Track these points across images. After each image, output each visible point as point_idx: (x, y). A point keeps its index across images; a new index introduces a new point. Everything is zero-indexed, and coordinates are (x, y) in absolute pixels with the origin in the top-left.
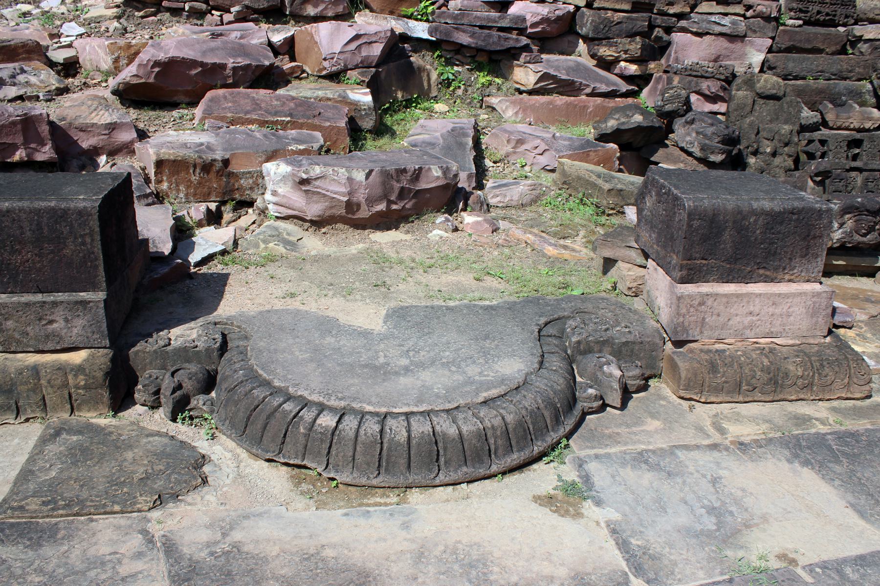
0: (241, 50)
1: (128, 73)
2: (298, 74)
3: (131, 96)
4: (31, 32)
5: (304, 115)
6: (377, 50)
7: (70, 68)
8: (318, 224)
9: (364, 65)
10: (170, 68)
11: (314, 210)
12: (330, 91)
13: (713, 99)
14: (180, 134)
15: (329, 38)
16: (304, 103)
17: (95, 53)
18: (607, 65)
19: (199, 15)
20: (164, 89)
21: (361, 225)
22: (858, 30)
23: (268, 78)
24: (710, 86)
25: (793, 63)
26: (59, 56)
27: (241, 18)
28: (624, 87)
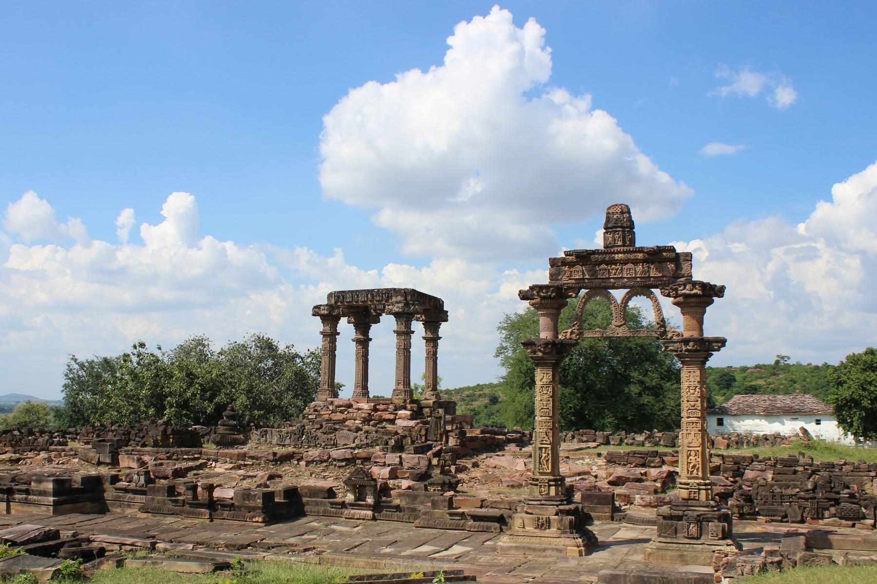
0: (634, 474)
1: (611, 479)
2: (647, 480)
3: (611, 483)
4: (586, 469)
5: (646, 488)
6: (665, 475)
7: (596, 477)
8: (644, 506)
9: (662, 478)
10: (619, 478)
11: (644, 503)
12: (652, 483)
13: (749, 486)
14: (618, 490)
15: (654, 472)
16: (646, 486)
17: (602, 473)
18: (727, 479)
19: (625, 465)
20: (618, 482)
21: (652, 507)
22: (796, 469)
23: (639, 480)
24: (749, 483)
25: (779, 477)
26: (594, 474)
27: (635, 466)
28: (730, 483)
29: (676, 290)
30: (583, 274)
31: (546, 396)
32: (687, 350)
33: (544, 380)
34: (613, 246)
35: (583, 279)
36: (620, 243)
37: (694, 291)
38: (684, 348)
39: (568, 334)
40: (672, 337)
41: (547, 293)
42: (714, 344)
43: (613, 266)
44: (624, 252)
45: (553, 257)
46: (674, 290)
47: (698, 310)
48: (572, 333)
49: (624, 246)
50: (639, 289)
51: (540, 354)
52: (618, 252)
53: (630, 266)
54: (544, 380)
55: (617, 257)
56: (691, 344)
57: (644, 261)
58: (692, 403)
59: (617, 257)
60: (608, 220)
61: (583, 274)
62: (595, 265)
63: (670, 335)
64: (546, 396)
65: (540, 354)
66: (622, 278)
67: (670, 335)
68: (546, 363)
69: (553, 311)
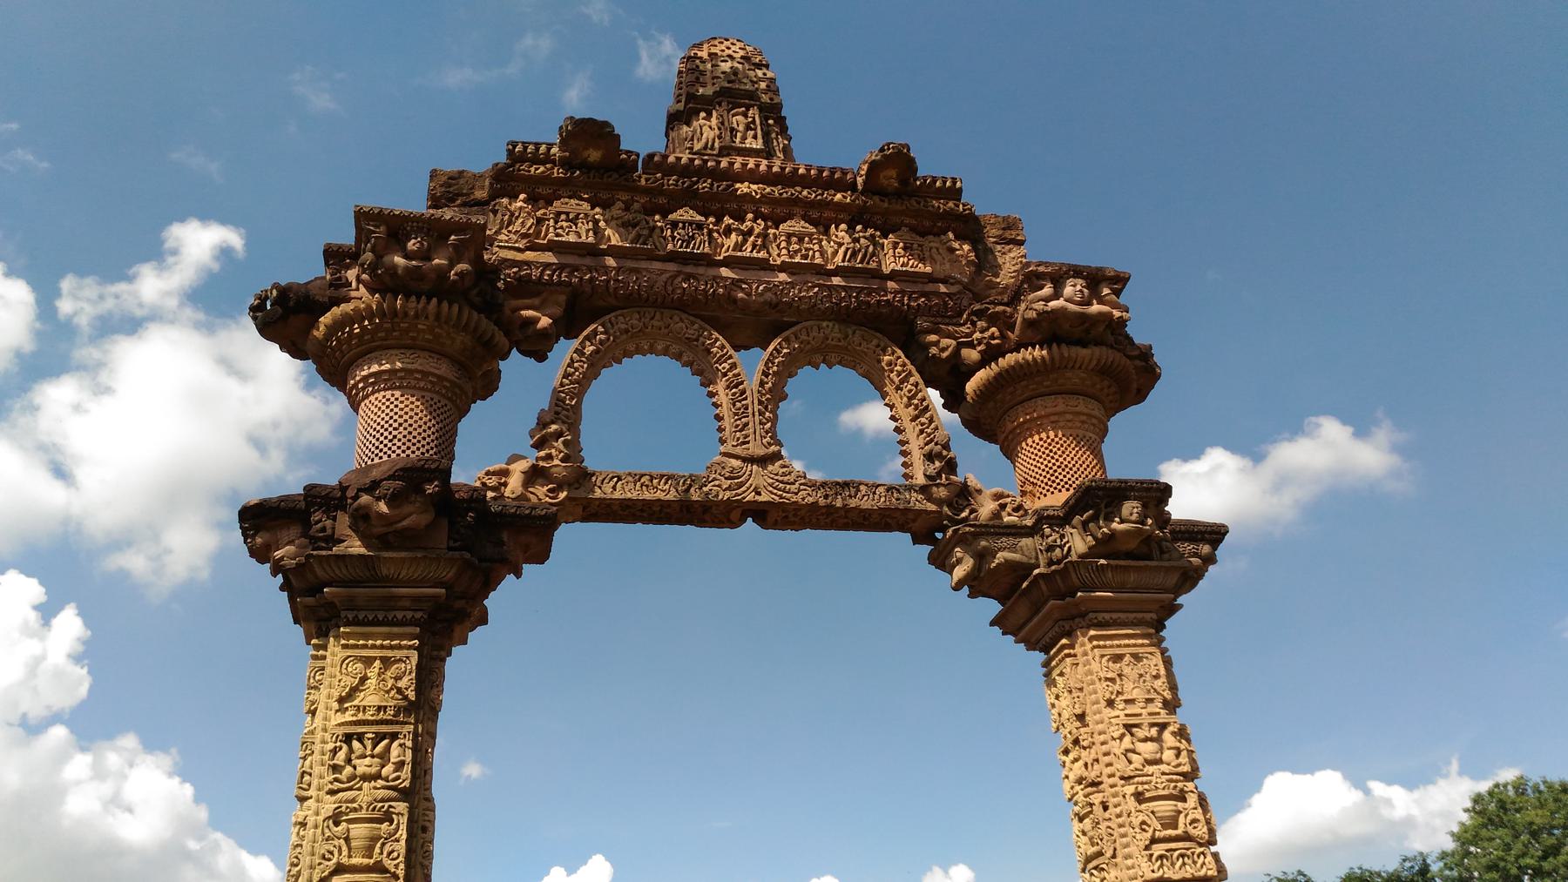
29: (1005, 323)
30: (597, 231)
31: (367, 793)
32: (1105, 546)
33: (370, 698)
34: (726, 151)
35: (592, 251)
36: (750, 143)
37: (1096, 308)
38: (1078, 543)
39: (514, 484)
40: (996, 515)
41: (425, 256)
42: (1187, 547)
43: (727, 220)
44: (769, 179)
45: (450, 166)
46: (993, 320)
47: (1094, 408)
48: (534, 475)
49: (768, 153)
50: (832, 330)
51: (356, 547)
52: (752, 176)
53: (796, 225)
54: (370, 698)
55: (743, 188)
56: (1131, 508)
57: (854, 217)
58: (1165, 807)
59: (743, 188)
60: (692, 70)
61: (597, 231)
62: (650, 211)
63: (986, 508)
64: (367, 793)
65: (356, 547)
66: (764, 265)
67: (986, 508)
68: (389, 603)
69: (443, 369)
